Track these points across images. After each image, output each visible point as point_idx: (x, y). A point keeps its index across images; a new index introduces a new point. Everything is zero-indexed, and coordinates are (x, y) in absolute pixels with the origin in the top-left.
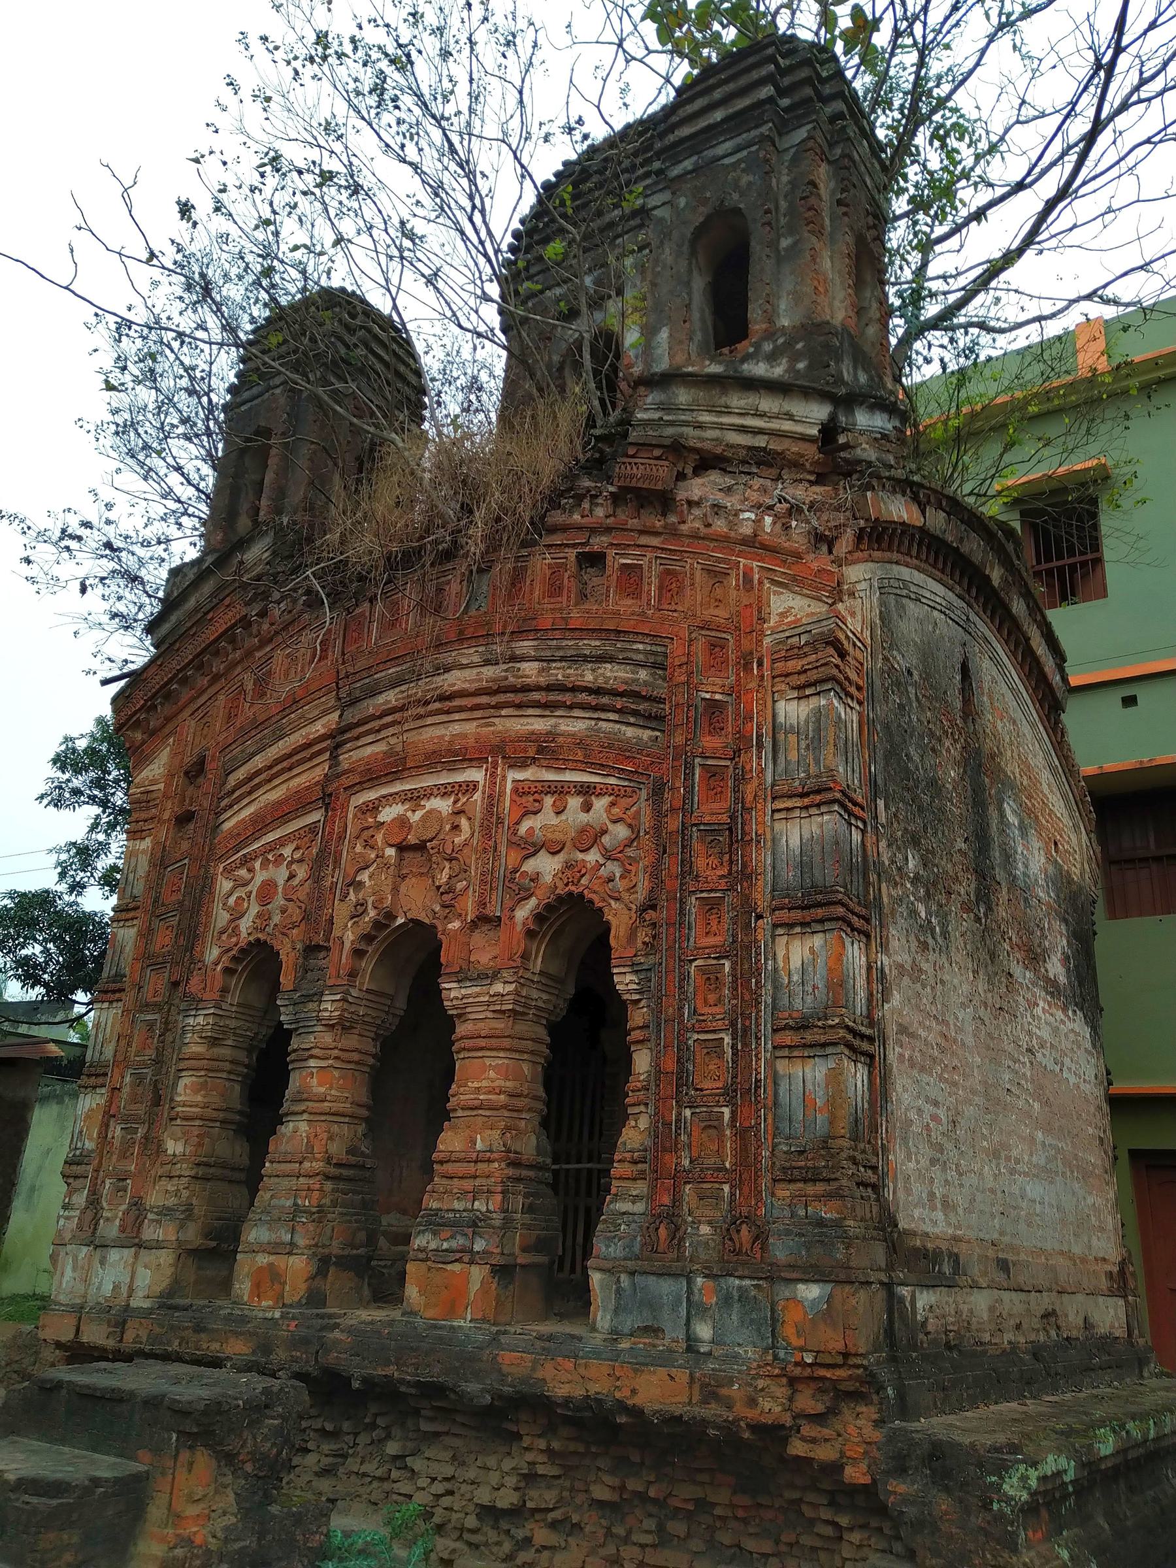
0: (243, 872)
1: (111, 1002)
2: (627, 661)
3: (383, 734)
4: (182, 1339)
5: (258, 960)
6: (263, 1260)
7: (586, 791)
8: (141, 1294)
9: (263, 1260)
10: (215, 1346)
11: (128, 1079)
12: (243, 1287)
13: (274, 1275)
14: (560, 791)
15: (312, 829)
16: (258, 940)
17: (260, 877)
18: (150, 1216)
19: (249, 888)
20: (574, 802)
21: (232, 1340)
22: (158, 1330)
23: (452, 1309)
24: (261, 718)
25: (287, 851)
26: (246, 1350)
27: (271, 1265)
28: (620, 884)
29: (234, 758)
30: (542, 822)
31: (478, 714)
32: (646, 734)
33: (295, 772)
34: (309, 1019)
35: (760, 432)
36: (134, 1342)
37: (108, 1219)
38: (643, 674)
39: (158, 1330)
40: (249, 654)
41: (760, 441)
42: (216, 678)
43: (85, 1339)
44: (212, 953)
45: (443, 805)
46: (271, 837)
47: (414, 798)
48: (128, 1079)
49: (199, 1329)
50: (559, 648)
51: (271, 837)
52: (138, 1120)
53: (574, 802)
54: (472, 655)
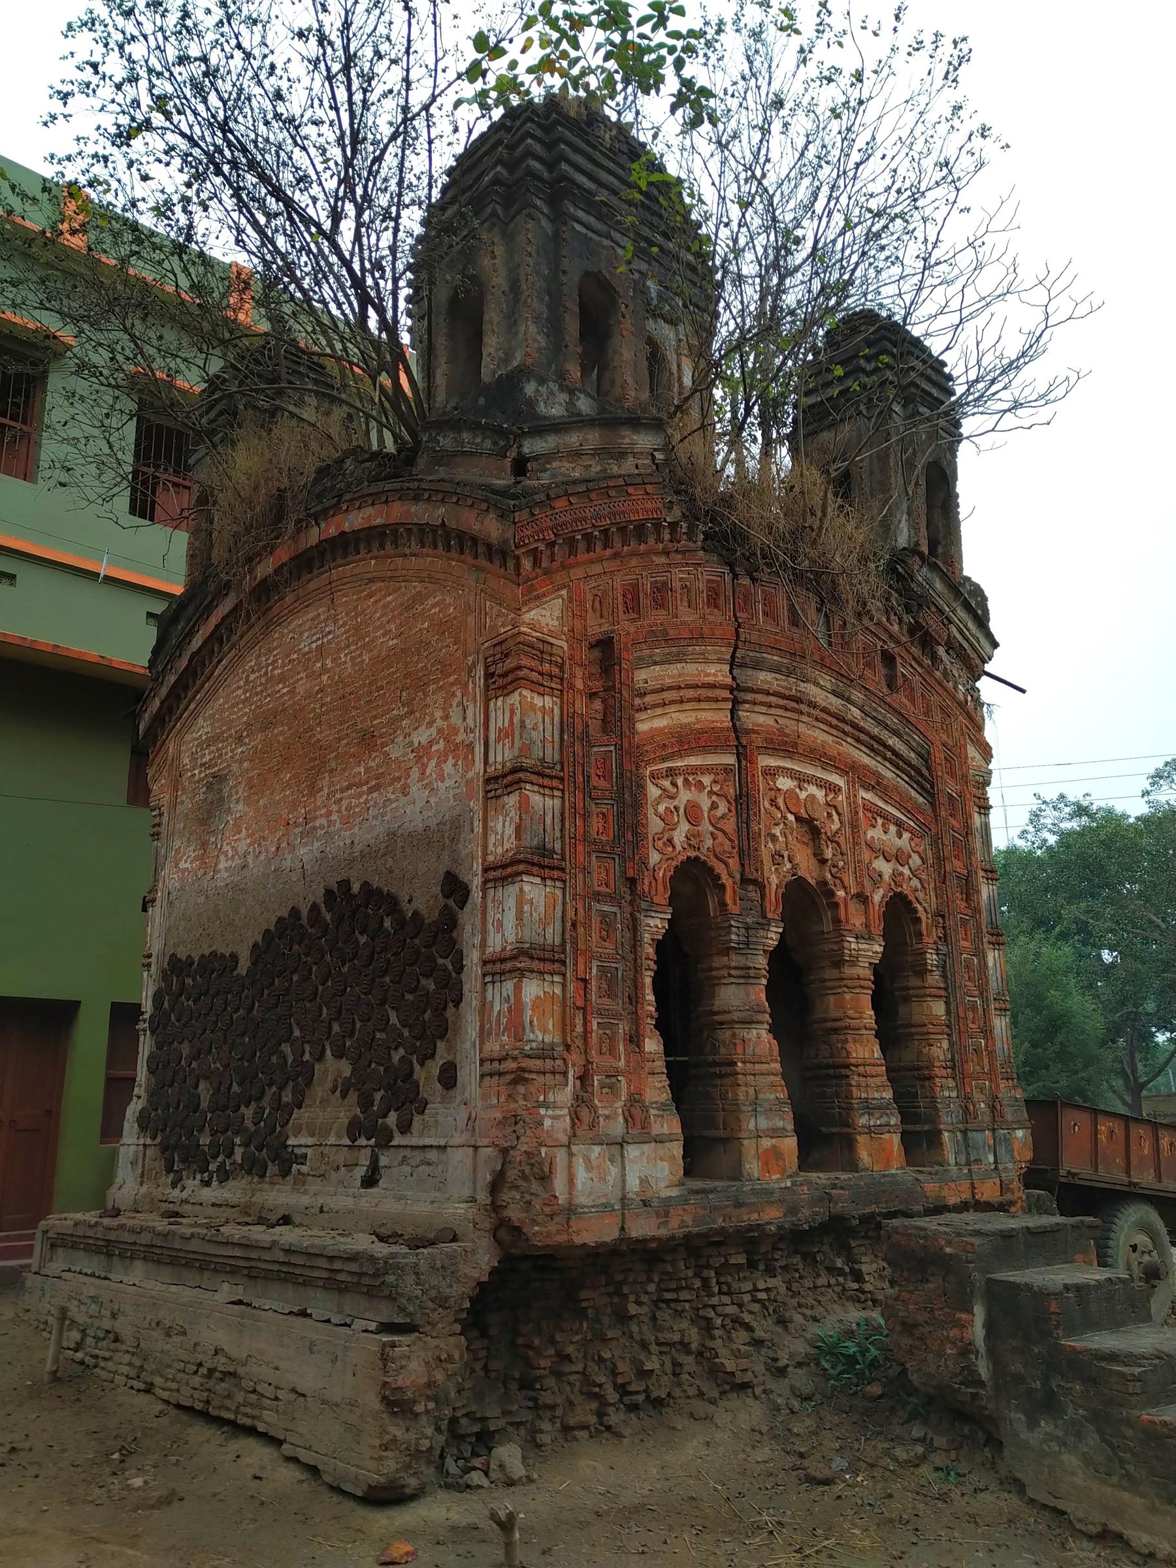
0: (666, 783)
1: (544, 879)
2: (907, 743)
3: (773, 711)
4: (725, 1216)
5: (693, 876)
6: (766, 1143)
7: (899, 824)
8: (662, 1185)
9: (766, 1143)
10: (755, 1216)
11: (594, 971)
12: (752, 1167)
13: (776, 1152)
14: (886, 817)
15: (727, 769)
16: (688, 858)
17: (685, 796)
18: (652, 1112)
19: (676, 803)
20: (906, 835)
21: (768, 1209)
22: (702, 1212)
23: (888, 1165)
24: (672, 633)
25: (706, 780)
26: (779, 1214)
27: (774, 1146)
28: (921, 895)
29: (640, 659)
30: (875, 834)
31: (835, 732)
32: (921, 799)
33: (704, 705)
34: (757, 943)
35: (967, 640)
36: (680, 1227)
37: (607, 1117)
38: (913, 755)
39: (702, 1212)
40: (648, 553)
41: (966, 645)
42: (616, 555)
43: (634, 1235)
44: (654, 858)
45: (820, 794)
46: (694, 761)
47: (802, 780)
48: (594, 971)
49: (739, 1205)
50: (875, 710)
51: (694, 761)
52: (617, 1016)
53: (893, 829)
54: (826, 680)
